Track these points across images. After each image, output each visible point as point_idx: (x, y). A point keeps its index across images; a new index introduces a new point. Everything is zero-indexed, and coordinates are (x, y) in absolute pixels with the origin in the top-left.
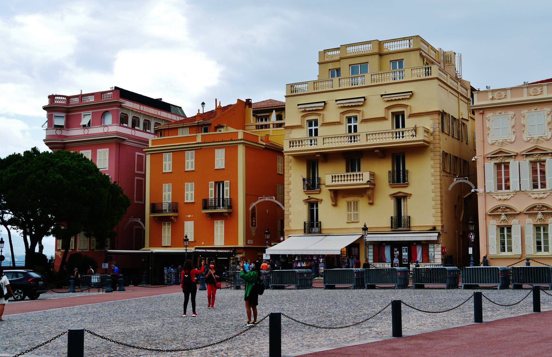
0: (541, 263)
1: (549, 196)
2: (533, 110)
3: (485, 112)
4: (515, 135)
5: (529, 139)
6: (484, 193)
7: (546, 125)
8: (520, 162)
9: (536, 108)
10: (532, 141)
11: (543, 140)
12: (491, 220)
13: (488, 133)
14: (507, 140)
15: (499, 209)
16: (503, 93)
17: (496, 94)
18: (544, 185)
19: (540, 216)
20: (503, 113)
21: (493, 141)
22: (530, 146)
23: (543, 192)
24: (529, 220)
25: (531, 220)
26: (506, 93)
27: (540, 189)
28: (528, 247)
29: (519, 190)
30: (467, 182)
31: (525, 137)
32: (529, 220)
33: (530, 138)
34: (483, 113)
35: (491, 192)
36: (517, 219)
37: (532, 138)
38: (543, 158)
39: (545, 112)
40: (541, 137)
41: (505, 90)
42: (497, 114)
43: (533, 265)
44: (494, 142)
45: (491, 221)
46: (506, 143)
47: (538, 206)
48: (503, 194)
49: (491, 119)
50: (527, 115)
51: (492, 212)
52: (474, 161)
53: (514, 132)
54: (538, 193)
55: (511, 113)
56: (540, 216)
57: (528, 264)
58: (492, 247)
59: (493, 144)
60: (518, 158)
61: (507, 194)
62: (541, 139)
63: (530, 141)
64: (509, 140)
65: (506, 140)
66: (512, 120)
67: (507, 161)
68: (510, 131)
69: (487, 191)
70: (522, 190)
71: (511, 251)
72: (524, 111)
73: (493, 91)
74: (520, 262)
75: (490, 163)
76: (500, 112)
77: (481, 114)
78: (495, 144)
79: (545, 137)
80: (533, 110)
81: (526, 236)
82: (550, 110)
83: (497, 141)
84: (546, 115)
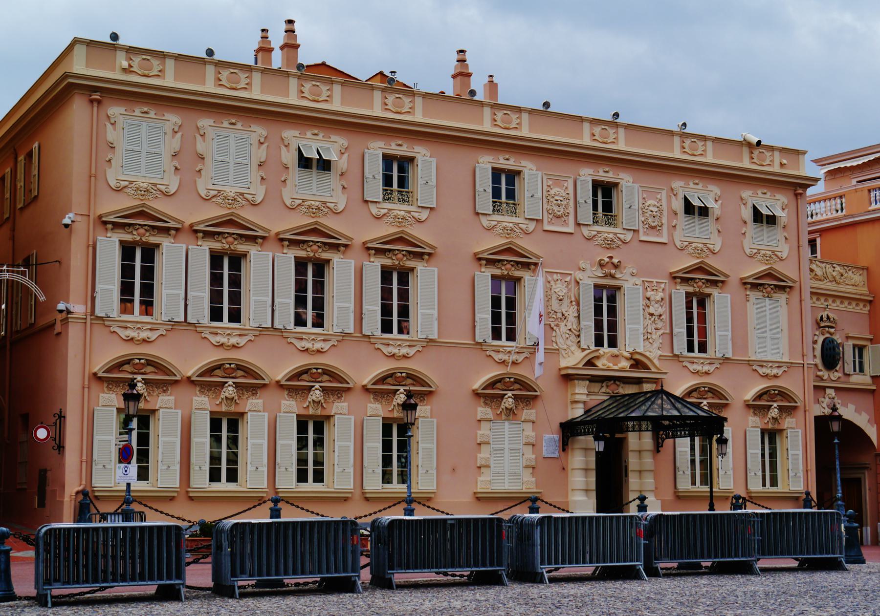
0: (312, 512)
1: (162, 338)
2: (226, 124)
3: (106, 102)
4: (179, 177)
5: (213, 193)
6: (89, 318)
7: (255, 166)
8: (190, 247)
9: (233, 121)
10: (218, 200)
11: (244, 203)
12: (103, 392)
13: (109, 157)
14: (158, 186)
15: (127, 365)
16: (155, 63)
17: (137, 60)
18: (235, 316)
19: (230, 391)
20: (152, 114)
21: (121, 182)
22: (215, 212)
23: (238, 332)
24: (374, 405)
25: (204, 399)
26: (164, 64)
27: (225, 323)
28: (197, 468)
29: (183, 321)
30: (25, 280)
31: (203, 186)
32: (288, 403)
33: (215, 193)
34: (99, 102)
35: (109, 317)
36: (171, 395)
37: (219, 191)
38: (241, 247)
39: (254, 135)
40: (242, 194)
41: (161, 55)
42: (137, 112)
43: (289, 515)
44: (124, 184)
45: (101, 395)
46: (154, 192)
47: (773, 392)
48: (139, 326)
49: (120, 121)
50: (210, 133)
51: (199, 376)
52: (67, 226)
53: (176, 168)
54: (229, 332)
55: (173, 118)
56: (230, 391)
57: (276, 513)
58: (102, 467)
59: (119, 190)
60: (182, 236)
61: (149, 327)
62: (239, 200)
63: (213, 200)
64: (163, 188)
65: (155, 185)
66: (173, 137)
67: (153, 240)
68: (167, 164)
69: (99, 312)
70: (190, 320)
71: (322, 481)
72: (205, 122)
73: (131, 51)
74: (251, 508)
75: (110, 237)
76: (145, 109)
77: (95, 104)
78: (126, 190)
79: (251, 196)
80: (226, 124)
81: (195, 440)
82: (264, 133)
83: (131, 182)
84: (256, 143)
